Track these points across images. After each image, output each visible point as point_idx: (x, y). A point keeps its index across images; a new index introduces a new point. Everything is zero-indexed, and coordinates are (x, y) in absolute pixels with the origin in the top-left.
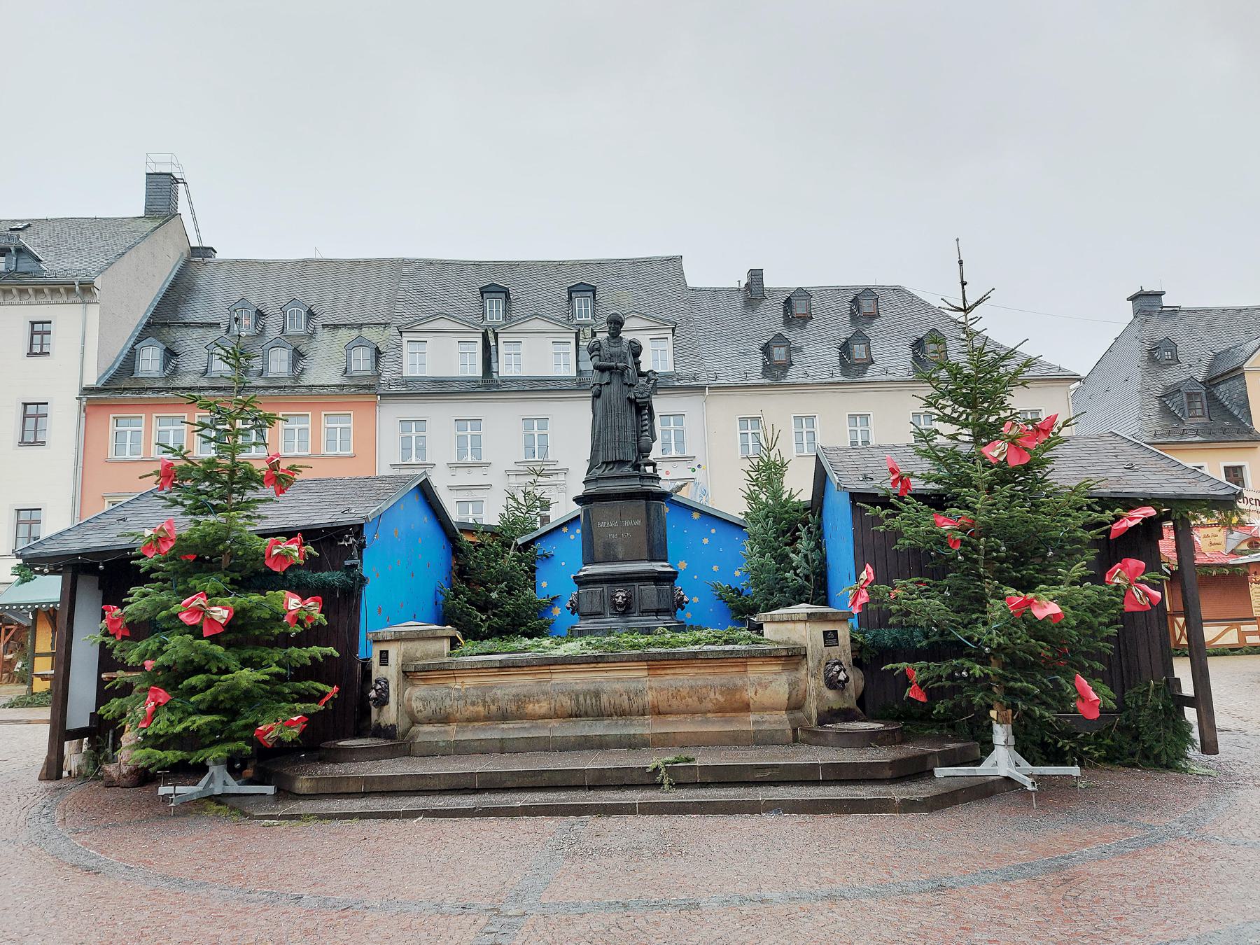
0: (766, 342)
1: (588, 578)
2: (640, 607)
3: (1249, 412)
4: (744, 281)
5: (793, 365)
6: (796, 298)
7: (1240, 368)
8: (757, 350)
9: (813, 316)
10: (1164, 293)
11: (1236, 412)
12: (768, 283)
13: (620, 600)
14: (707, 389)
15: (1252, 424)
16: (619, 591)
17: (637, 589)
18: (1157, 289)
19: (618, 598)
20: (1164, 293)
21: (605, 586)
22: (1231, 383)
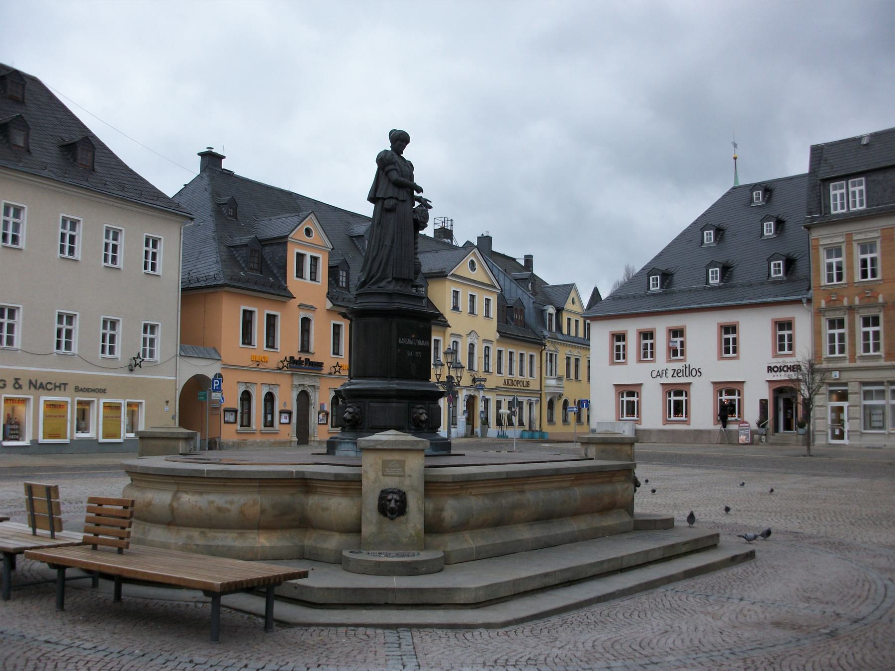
3: (285, 273)
7: (286, 237)
10: (224, 157)
11: (275, 271)
15: (286, 283)
18: (220, 153)
20: (224, 157)
22: (275, 247)
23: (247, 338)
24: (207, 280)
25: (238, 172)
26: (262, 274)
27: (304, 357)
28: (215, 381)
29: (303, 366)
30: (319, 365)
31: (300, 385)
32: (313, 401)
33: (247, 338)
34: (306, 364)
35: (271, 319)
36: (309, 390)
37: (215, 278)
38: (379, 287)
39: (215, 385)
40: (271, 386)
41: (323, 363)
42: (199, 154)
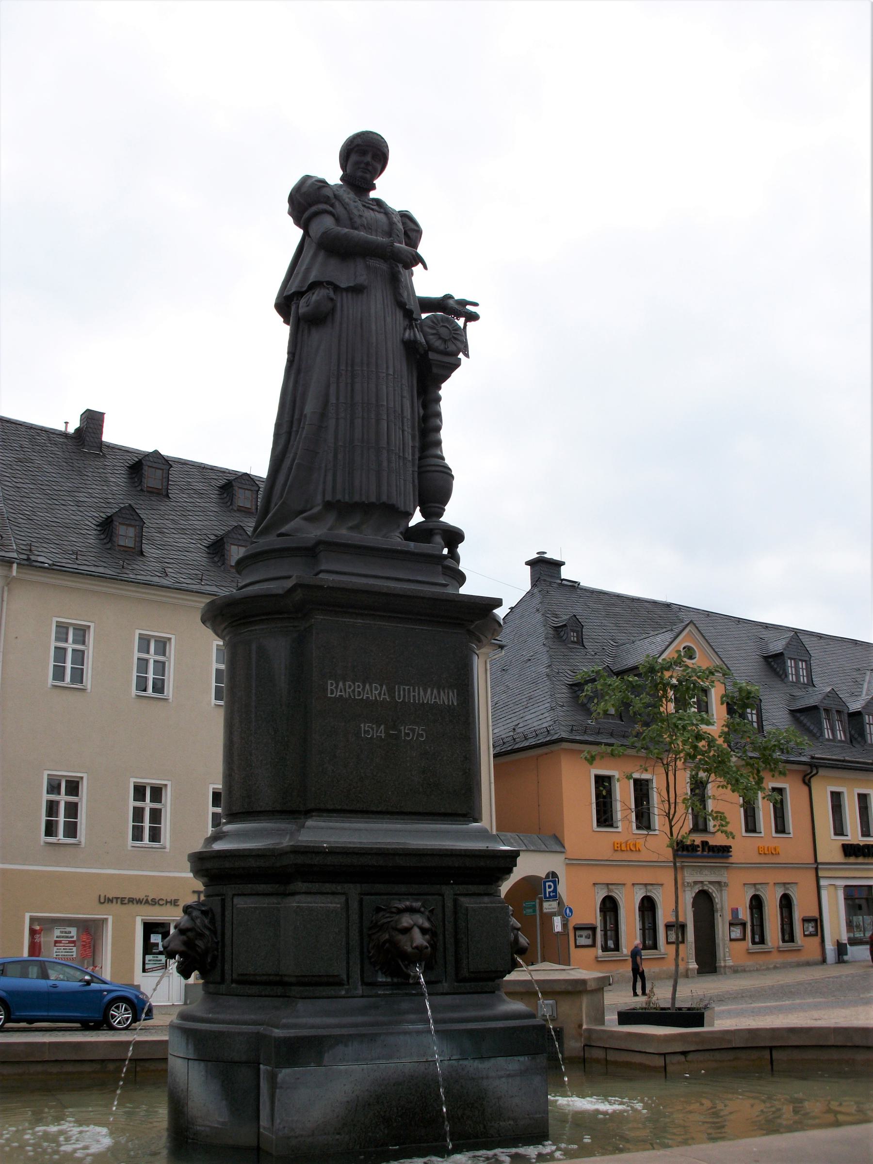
0: (109, 515)
1: (300, 860)
2: (458, 961)
4: (74, 425)
5: (144, 556)
6: (149, 464)
8: (90, 524)
9: (170, 495)
10: (563, 564)
12: (111, 435)
13: (419, 939)
14: (15, 566)
16: (411, 910)
17: (449, 904)
19: (407, 931)
20: (563, 564)
21: (354, 890)
23: (605, 816)
24: (537, 735)
25: (586, 582)
26: (622, 721)
27: (698, 839)
28: (547, 884)
29: (699, 853)
30: (725, 850)
31: (696, 883)
32: (719, 906)
33: (605, 816)
34: (703, 850)
35: (642, 789)
36: (712, 889)
37: (548, 731)
38: (279, 535)
39: (548, 890)
40: (649, 887)
41: (730, 847)
42: (527, 563)
